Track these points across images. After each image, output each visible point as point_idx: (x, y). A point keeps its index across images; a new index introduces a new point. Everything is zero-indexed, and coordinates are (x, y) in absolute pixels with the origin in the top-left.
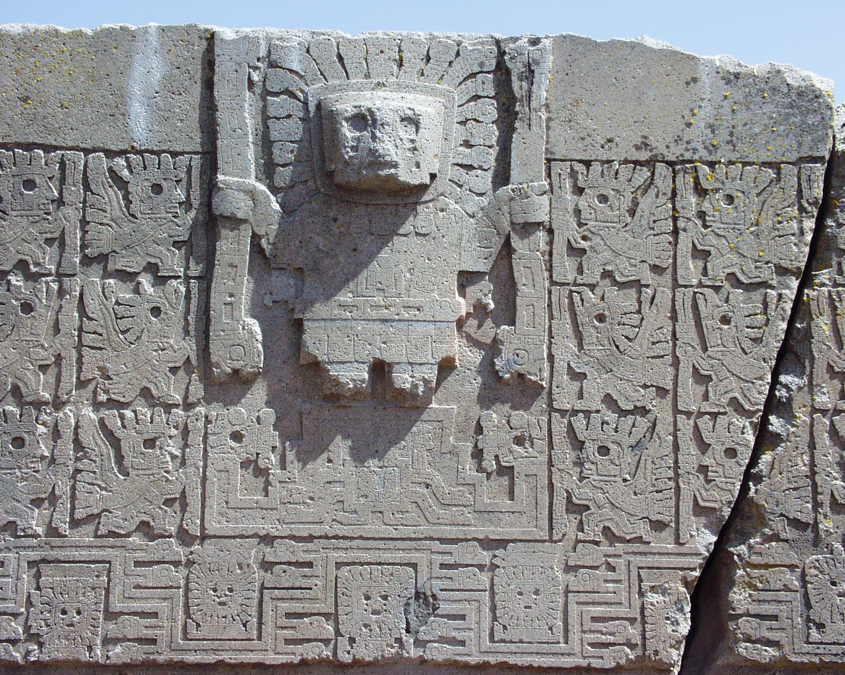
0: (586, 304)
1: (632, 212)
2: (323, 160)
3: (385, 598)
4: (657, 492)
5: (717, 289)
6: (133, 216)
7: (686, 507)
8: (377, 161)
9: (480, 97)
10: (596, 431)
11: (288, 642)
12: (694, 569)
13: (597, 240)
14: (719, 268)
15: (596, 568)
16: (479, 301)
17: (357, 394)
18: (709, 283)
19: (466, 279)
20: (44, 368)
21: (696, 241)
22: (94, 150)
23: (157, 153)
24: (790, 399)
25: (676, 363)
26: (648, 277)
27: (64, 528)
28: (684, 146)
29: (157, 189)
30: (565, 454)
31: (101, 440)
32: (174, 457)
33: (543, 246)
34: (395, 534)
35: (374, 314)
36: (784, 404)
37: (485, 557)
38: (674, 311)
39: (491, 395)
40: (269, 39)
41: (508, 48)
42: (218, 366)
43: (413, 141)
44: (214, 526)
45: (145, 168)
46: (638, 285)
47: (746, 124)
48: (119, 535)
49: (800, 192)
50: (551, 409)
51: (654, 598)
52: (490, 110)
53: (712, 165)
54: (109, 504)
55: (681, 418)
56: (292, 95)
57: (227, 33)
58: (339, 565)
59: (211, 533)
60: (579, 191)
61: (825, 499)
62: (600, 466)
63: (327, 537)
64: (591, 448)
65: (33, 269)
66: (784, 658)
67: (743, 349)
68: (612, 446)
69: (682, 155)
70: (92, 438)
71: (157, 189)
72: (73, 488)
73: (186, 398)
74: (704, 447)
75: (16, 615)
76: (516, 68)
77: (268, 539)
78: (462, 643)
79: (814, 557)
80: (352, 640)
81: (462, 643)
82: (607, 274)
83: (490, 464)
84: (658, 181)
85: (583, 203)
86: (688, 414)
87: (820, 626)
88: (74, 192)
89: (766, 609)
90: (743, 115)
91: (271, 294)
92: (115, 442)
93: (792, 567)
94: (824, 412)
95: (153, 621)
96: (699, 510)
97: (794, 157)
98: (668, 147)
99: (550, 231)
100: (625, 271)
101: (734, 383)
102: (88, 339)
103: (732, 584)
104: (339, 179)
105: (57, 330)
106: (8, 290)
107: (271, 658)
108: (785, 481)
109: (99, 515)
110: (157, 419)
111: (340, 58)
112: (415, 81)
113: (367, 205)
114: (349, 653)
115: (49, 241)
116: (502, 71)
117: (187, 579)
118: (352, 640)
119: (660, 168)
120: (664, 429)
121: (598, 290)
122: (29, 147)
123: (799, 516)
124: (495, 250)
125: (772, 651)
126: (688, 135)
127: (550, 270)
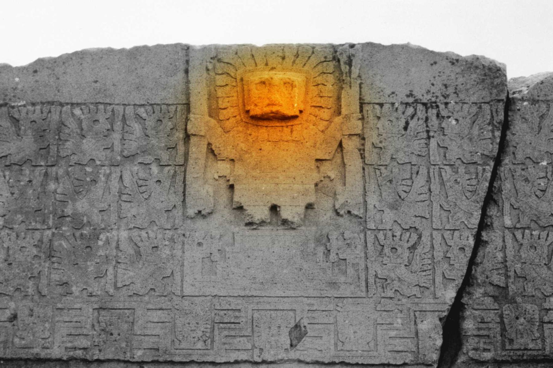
0: (383, 176)
1: (406, 128)
2: (244, 105)
4: (423, 271)
6: (147, 136)
7: (439, 279)
9: (325, 73)
12: (444, 311)
18: (447, 163)
21: (439, 142)
26: (414, 160)
28: (431, 95)
34: (283, 295)
36: (489, 226)
39: (334, 223)
44: (188, 291)
45: (154, 112)
47: (463, 84)
52: (331, 79)
54: (134, 279)
55: (435, 233)
59: (186, 295)
61: (512, 274)
62: (392, 259)
67: (466, 196)
69: (430, 99)
76: (344, 58)
79: (507, 305)
84: (419, 113)
87: (511, 341)
88: (118, 125)
89: (482, 332)
90: (461, 80)
91: (218, 172)
97: (488, 99)
98: (423, 95)
103: (464, 318)
104: (252, 113)
108: (490, 265)
111: (253, 56)
113: (267, 127)
114: (259, 356)
121: (389, 168)
123: (498, 283)
126: (433, 89)
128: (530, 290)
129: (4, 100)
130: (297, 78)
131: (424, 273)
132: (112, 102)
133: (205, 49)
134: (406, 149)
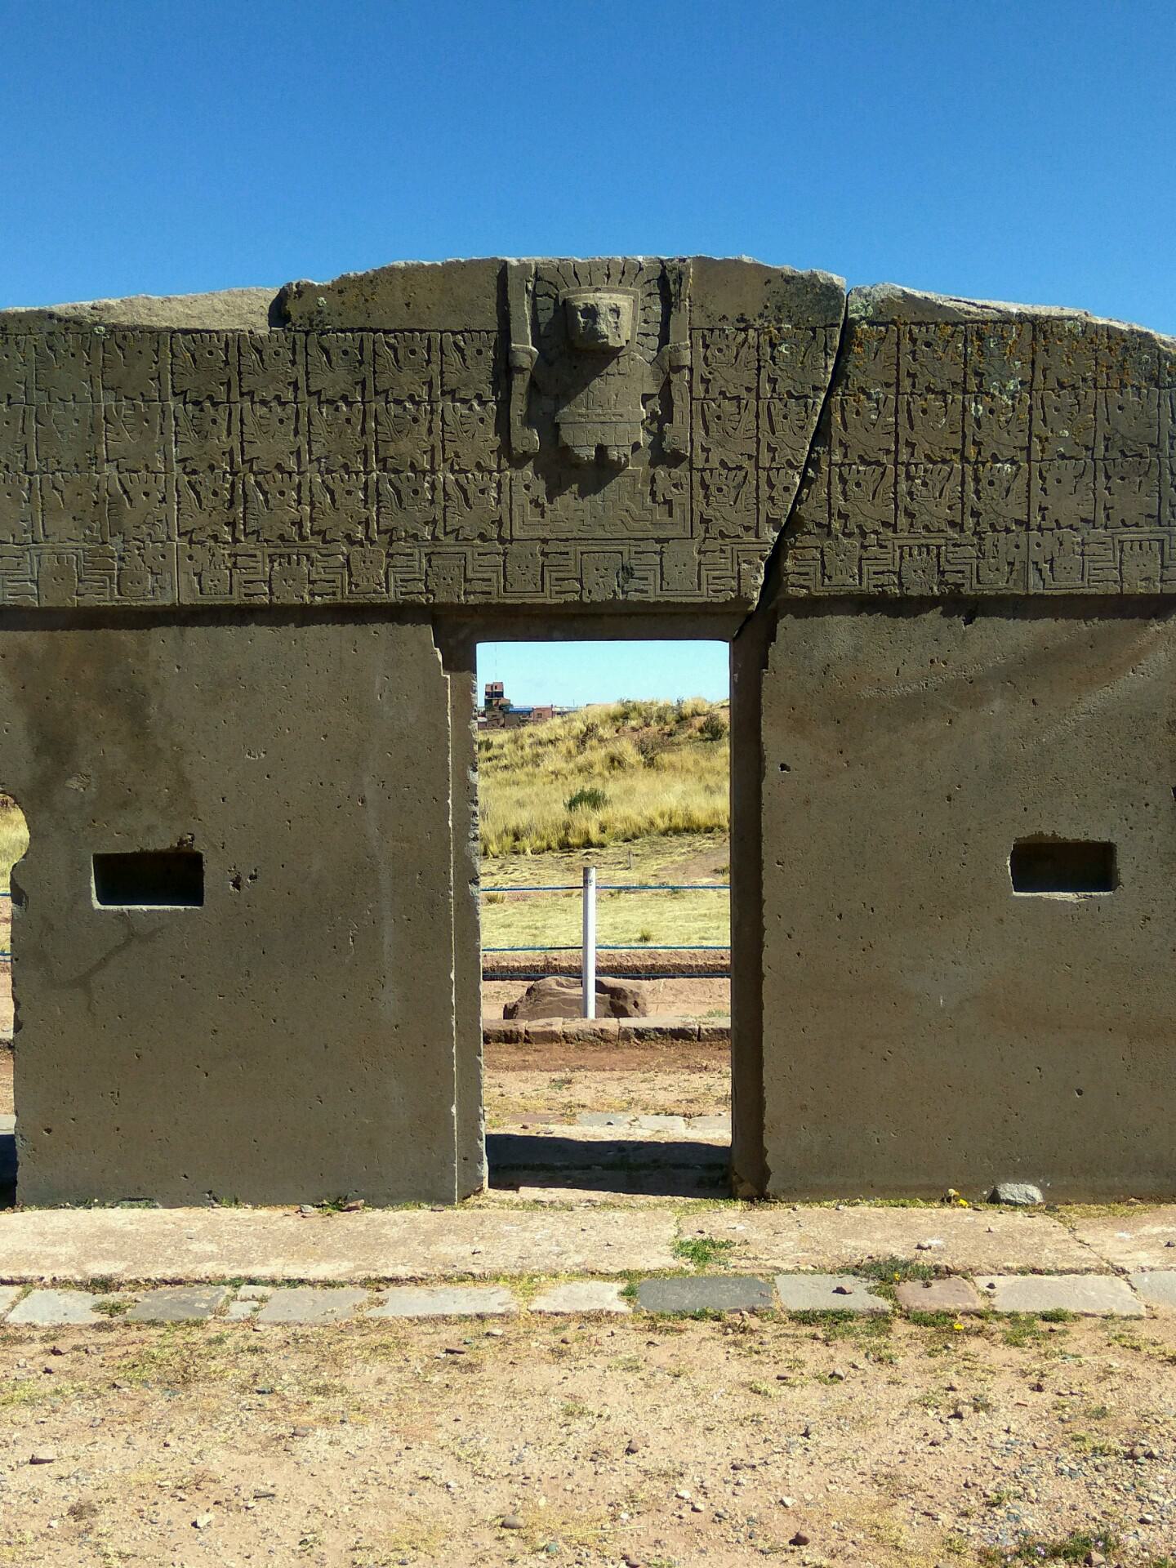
3: (606, 569)
5: (780, 399)
7: (762, 518)
8: (595, 334)
10: (716, 480)
11: (557, 593)
13: (716, 373)
14: (782, 387)
15: (715, 551)
16: (654, 410)
17: (589, 462)
19: (646, 398)
20: (425, 452)
22: (445, 331)
23: (479, 332)
24: (819, 458)
26: (744, 394)
27: (442, 536)
29: (479, 352)
30: (699, 493)
32: (494, 498)
33: (687, 378)
34: (609, 535)
35: (597, 419)
37: (658, 546)
38: (757, 412)
40: (536, 264)
42: (515, 449)
43: (616, 323)
44: (517, 534)
46: (738, 398)
48: (468, 540)
49: (826, 343)
50: (691, 469)
51: (745, 566)
56: (550, 297)
57: (513, 261)
58: (582, 553)
60: (706, 346)
63: (575, 539)
65: (417, 399)
66: (810, 594)
68: (724, 487)
70: (453, 490)
71: (479, 352)
72: (444, 515)
73: (499, 466)
74: (771, 486)
75: (421, 580)
76: (672, 277)
77: (545, 541)
78: (646, 592)
80: (590, 592)
81: (646, 592)
82: (722, 393)
84: (750, 340)
85: (709, 353)
86: (764, 469)
88: (436, 356)
89: (803, 570)
92: (464, 492)
93: (816, 548)
94: (836, 465)
95: (489, 583)
96: (769, 520)
99: (691, 370)
100: (732, 391)
101: (789, 451)
102: (447, 436)
105: (430, 431)
106: (405, 410)
107: (549, 601)
109: (458, 530)
110: (485, 478)
115: (424, 383)
116: (663, 281)
117: (504, 561)
118: (590, 592)
119: (751, 332)
121: (718, 402)
122: (411, 331)
124: (661, 382)
127: (691, 392)
128: (852, 526)
129: (311, 325)
130: (623, 301)
131: (748, 513)
132: (428, 328)
133: (524, 267)
134: (735, 381)
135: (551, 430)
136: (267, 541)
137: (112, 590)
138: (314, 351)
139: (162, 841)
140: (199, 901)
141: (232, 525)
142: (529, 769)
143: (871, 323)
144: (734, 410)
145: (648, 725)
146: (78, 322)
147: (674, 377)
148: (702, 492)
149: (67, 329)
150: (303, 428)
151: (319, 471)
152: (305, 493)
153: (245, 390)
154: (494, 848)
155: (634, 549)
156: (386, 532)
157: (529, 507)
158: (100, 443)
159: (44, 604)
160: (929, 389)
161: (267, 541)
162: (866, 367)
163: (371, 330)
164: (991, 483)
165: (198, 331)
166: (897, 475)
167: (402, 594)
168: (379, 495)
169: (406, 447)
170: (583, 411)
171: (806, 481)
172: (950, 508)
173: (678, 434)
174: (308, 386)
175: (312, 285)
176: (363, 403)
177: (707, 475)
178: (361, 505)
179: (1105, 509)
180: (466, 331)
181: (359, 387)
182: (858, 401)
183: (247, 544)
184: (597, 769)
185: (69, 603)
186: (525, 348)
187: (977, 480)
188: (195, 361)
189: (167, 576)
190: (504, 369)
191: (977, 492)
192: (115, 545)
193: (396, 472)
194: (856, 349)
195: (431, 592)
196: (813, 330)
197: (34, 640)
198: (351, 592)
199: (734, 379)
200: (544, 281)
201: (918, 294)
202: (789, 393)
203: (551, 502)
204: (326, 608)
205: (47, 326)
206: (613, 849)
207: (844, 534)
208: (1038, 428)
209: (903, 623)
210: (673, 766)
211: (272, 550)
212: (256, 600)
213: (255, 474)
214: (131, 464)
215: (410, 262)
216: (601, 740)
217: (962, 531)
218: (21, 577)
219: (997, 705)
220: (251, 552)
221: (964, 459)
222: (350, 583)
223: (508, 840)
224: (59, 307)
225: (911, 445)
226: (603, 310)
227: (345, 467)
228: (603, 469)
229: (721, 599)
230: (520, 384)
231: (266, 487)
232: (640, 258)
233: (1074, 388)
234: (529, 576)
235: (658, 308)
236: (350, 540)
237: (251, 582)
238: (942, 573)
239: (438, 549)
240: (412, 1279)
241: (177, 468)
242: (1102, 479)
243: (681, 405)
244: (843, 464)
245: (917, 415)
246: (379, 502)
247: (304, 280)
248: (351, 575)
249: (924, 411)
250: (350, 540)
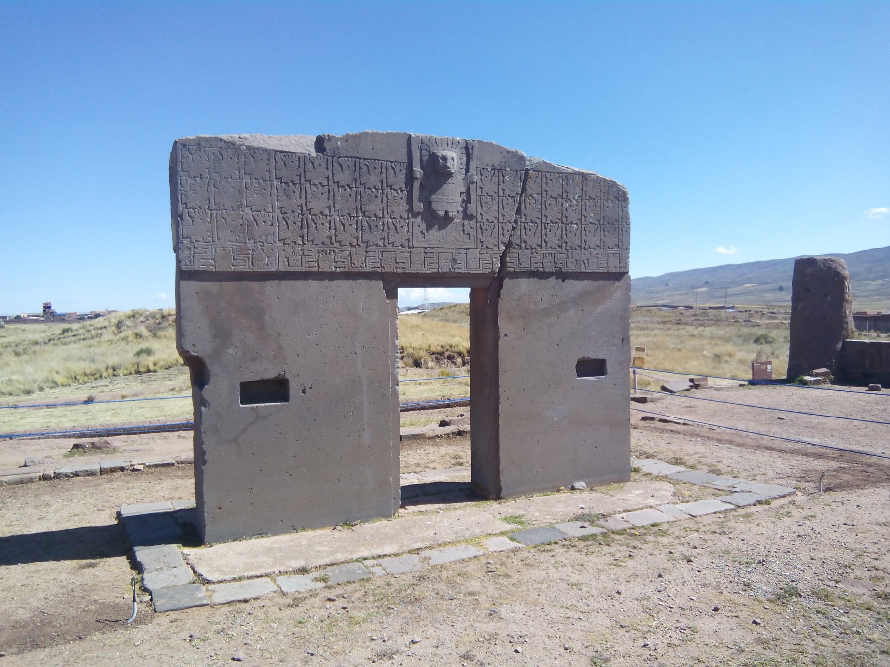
7: (500, 241)
8: (446, 167)
14: (507, 192)
19: (462, 193)
23: (400, 162)
25: (499, 213)
26: (494, 194)
27: (387, 245)
29: (401, 170)
30: (479, 231)
31: (392, 226)
41: (468, 142)
44: (415, 245)
46: (492, 196)
50: (477, 222)
51: (494, 259)
53: (505, 170)
60: (481, 175)
64: (484, 230)
70: (391, 226)
71: (401, 170)
74: (503, 230)
76: (470, 147)
77: (425, 248)
82: (487, 193)
83: (466, 233)
88: (384, 170)
89: (513, 261)
92: (395, 227)
96: (502, 242)
102: (389, 204)
112: (451, 148)
116: (467, 148)
120: (497, 226)
122: (375, 160)
125: (513, 269)
126: (501, 164)
133: (417, 137)
135: (428, 204)
136: (317, 244)
137: (249, 263)
138: (335, 164)
139: (271, 374)
140: (288, 401)
141: (302, 237)
142: (97, 340)
143: (534, 171)
144: (491, 200)
145: (148, 320)
146: (233, 144)
147: (471, 186)
148: (480, 231)
149: (228, 146)
150: (331, 197)
151: (338, 216)
152: (332, 225)
153: (307, 179)
154: (105, 374)
155: (457, 252)
156: (365, 242)
157: (420, 234)
158: (243, 198)
159: (218, 269)
160: (552, 197)
161: (317, 244)
162: (533, 188)
163: (358, 158)
164: (570, 232)
165: (286, 152)
166: (542, 227)
167: (372, 268)
168: (362, 226)
169: (374, 207)
170: (440, 197)
171: (514, 228)
172: (558, 240)
173: (472, 208)
174: (333, 180)
175: (334, 137)
176: (356, 188)
177: (482, 224)
178: (355, 231)
179: (604, 242)
180: (396, 161)
181: (354, 181)
182: (530, 199)
183: (308, 245)
184: (130, 339)
185: (229, 270)
186: (418, 170)
187: (566, 230)
188: (285, 165)
189: (274, 258)
190: (410, 178)
191: (566, 235)
192: (250, 244)
193: (369, 217)
194: (529, 180)
195: (382, 267)
196: (516, 172)
197: (212, 286)
198: (351, 267)
199: (490, 188)
200: (424, 143)
201: (548, 162)
202: (509, 195)
203: (427, 232)
204: (341, 273)
205: (220, 144)
206: (161, 373)
207: (525, 248)
208: (584, 213)
209: (543, 281)
210: (165, 337)
211: (319, 249)
212: (312, 270)
213: (311, 215)
214: (257, 208)
215: (374, 131)
216: (128, 327)
217: (562, 248)
218: (207, 257)
219: (572, 311)
220: (310, 249)
221: (562, 223)
222: (351, 263)
223: (111, 371)
224: (224, 137)
225: (546, 217)
226: (449, 158)
227: (349, 214)
228: (447, 220)
229: (486, 272)
230: (417, 185)
231: (316, 221)
232: (458, 139)
233: (594, 199)
234: (420, 262)
235: (465, 158)
236: (351, 245)
237: (311, 262)
238: (556, 263)
239: (385, 250)
240: (426, 548)
241: (278, 211)
242: (602, 232)
243: (473, 197)
244: (525, 223)
245: (548, 205)
246: (362, 229)
247: (331, 134)
248: (351, 260)
249: (550, 205)
250: (351, 245)
